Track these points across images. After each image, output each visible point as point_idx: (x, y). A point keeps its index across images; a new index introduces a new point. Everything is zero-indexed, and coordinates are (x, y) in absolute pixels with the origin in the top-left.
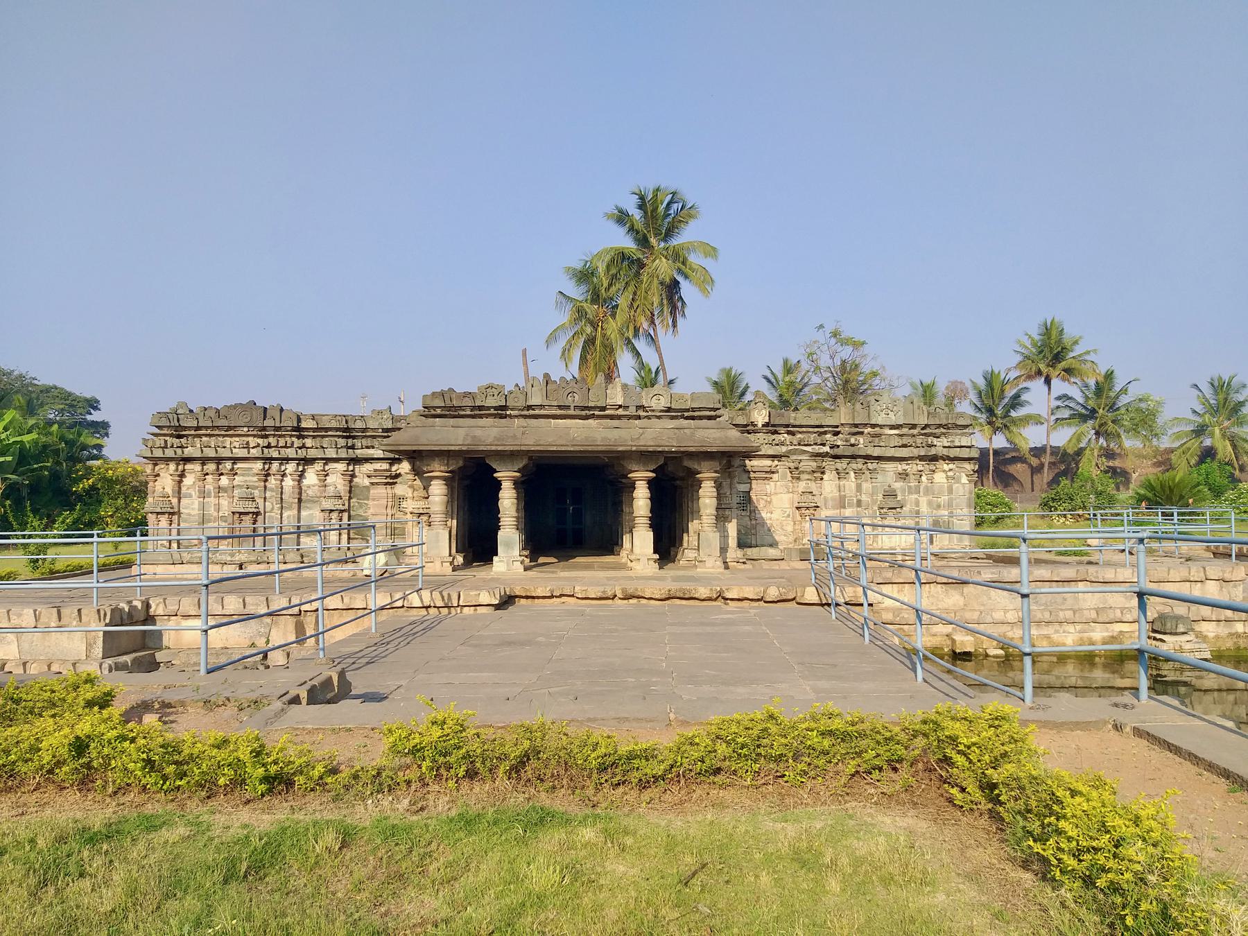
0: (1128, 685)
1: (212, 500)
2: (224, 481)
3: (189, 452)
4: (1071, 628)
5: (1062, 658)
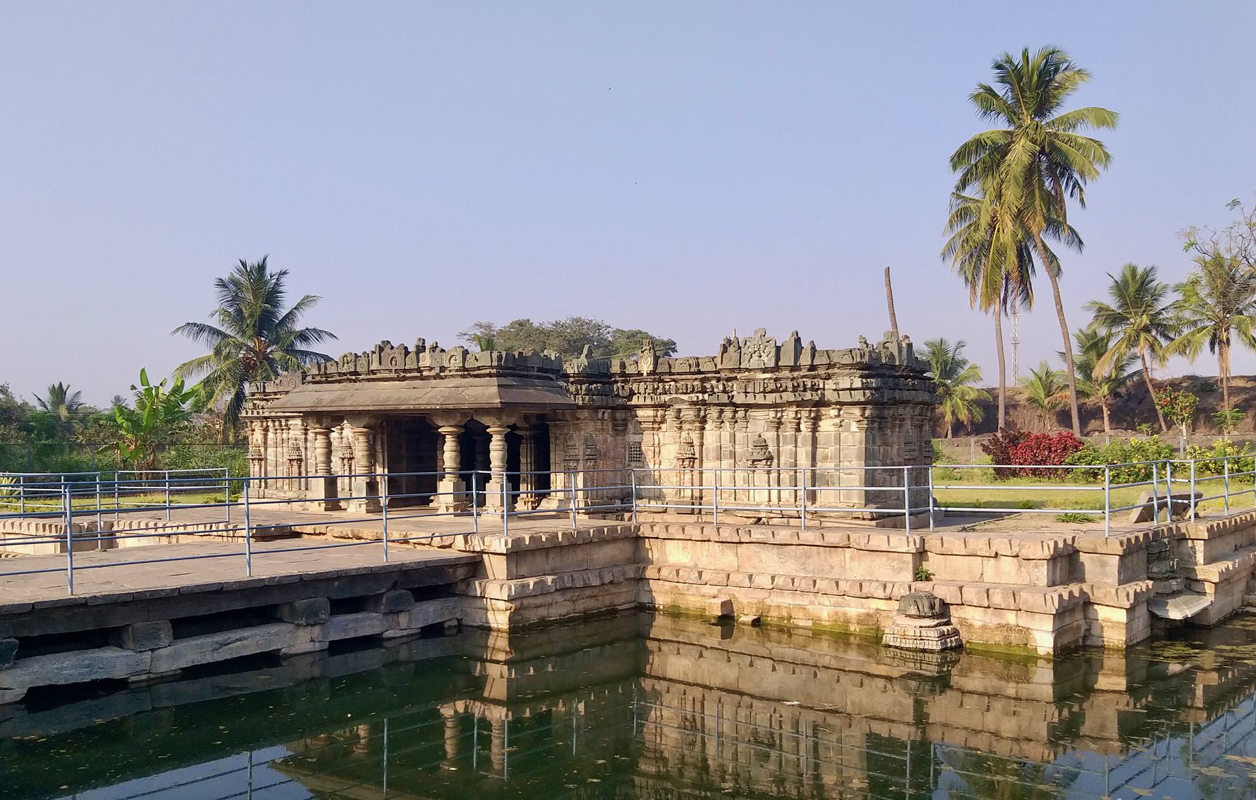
0: (884, 674)
1: (279, 449)
2: (285, 436)
3: (266, 414)
4: (825, 600)
5: (817, 634)
